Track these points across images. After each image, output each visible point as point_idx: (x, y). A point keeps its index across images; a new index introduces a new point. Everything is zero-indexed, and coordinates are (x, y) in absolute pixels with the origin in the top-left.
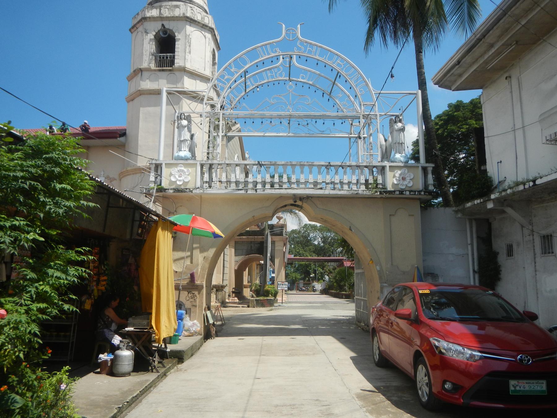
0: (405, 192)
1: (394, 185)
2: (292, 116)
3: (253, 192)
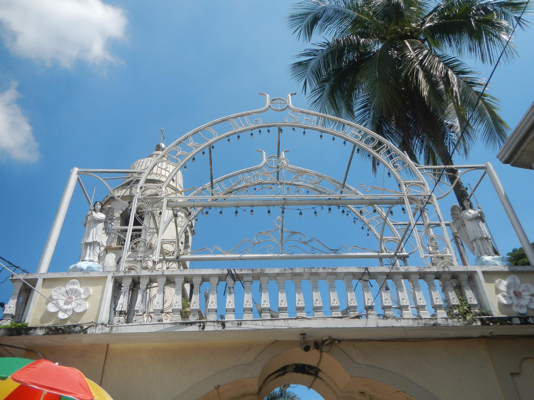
0: (530, 319)
1: (501, 306)
2: (288, 201)
3: (217, 328)
